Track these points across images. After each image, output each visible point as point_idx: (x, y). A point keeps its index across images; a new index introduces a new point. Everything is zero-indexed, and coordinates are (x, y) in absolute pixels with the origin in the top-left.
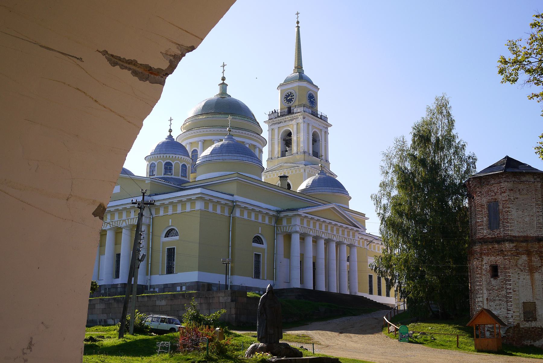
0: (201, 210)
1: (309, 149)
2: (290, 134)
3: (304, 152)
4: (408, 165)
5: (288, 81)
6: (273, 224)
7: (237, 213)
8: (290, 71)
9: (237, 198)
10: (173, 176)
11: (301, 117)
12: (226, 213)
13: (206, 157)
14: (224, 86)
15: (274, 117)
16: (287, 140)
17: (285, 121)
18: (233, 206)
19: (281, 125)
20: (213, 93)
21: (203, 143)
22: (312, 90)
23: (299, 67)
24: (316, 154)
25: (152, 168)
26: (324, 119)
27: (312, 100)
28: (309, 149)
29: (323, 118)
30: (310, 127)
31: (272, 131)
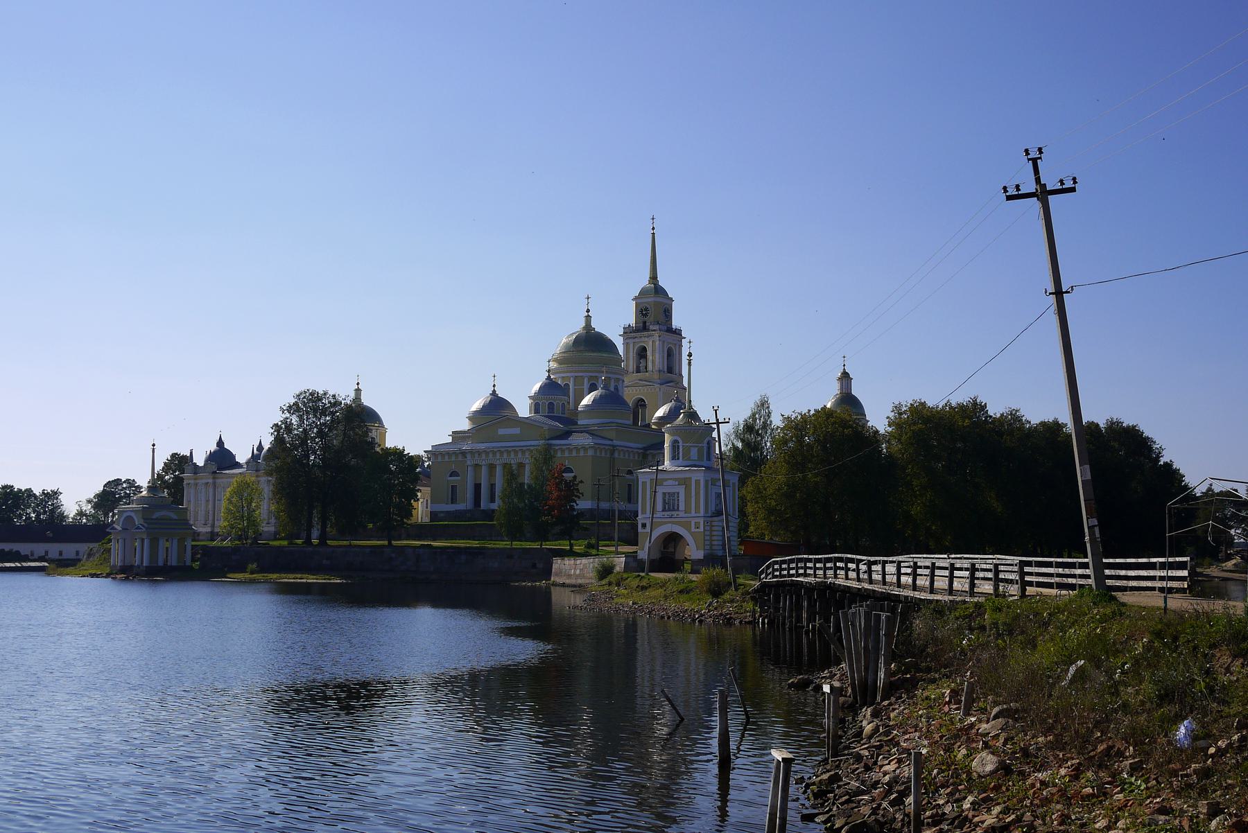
0: (592, 456)
1: (663, 368)
2: (644, 349)
3: (660, 371)
4: (740, 445)
5: (643, 292)
6: (641, 459)
7: (616, 455)
8: (644, 281)
9: (616, 442)
10: (555, 415)
11: (658, 335)
12: (608, 456)
13: (587, 406)
14: (588, 318)
15: (628, 332)
16: (642, 354)
17: (641, 337)
18: (613, 449)
19: (636, 340)
20: (578, 326)
21: (575, 379)
22: (666, 304)
23: (654, 278)
24: (670, 370)
25: (536, 408)
26: (678, 332)
27: (667, 313)
28: (663, 368)
29: (677, 331)
30: (665, 343)
31: (626, 345)
